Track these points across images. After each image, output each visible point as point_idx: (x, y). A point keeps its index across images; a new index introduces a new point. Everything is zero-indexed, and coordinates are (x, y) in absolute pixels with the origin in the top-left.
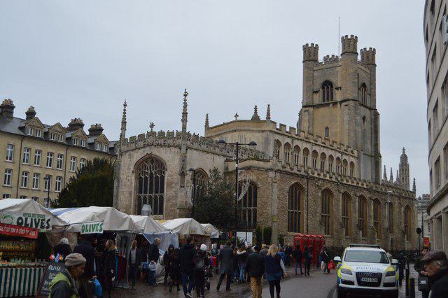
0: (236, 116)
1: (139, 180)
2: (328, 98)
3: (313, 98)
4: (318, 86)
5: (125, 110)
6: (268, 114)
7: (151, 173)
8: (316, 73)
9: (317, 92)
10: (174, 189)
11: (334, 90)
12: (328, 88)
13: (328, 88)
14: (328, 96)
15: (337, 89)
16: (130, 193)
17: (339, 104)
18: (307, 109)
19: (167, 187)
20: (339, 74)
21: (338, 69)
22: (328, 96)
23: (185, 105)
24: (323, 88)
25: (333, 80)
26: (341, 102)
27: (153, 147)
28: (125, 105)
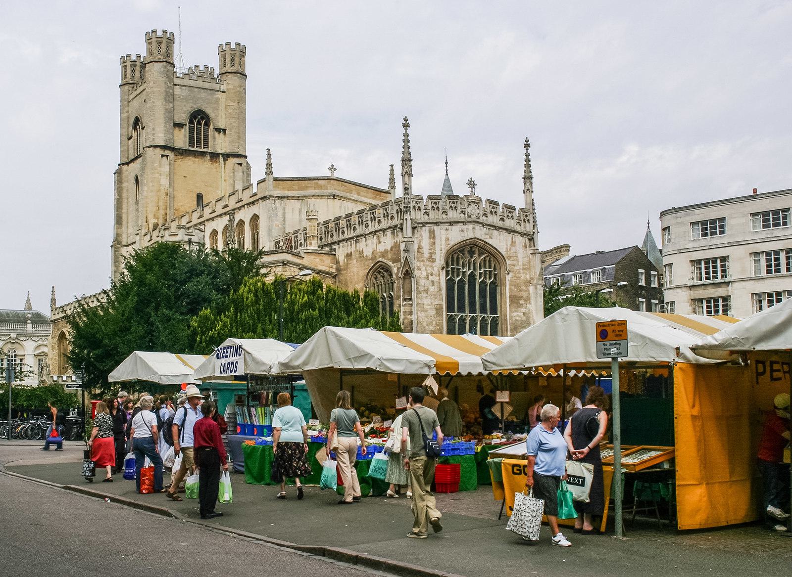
0: (332, 168)
1: (450, 283)
2: (199, 142)
3: (173, 135)
4: (182, 117)
5: (406, 135)
6: (269, 166)
7: (472, 276)
8: (177, 90)
9: (179, 126)
10: (523, 310)
11: (211, 132)
12: (199, 123)
13: (199, 123)
14: (199, 138)
15: (218, 130)
16: (438, 310)
17: (221, 159)
18: (167, 152)
19: (512, 302)
20: (222, 106)
21: (220, 95)
22: (199, 138)
23: (406, 141)
24: (191, 122)
25: (209, 111)
26: (226, 156)
27: (477, 227)
28: (406, 126)
